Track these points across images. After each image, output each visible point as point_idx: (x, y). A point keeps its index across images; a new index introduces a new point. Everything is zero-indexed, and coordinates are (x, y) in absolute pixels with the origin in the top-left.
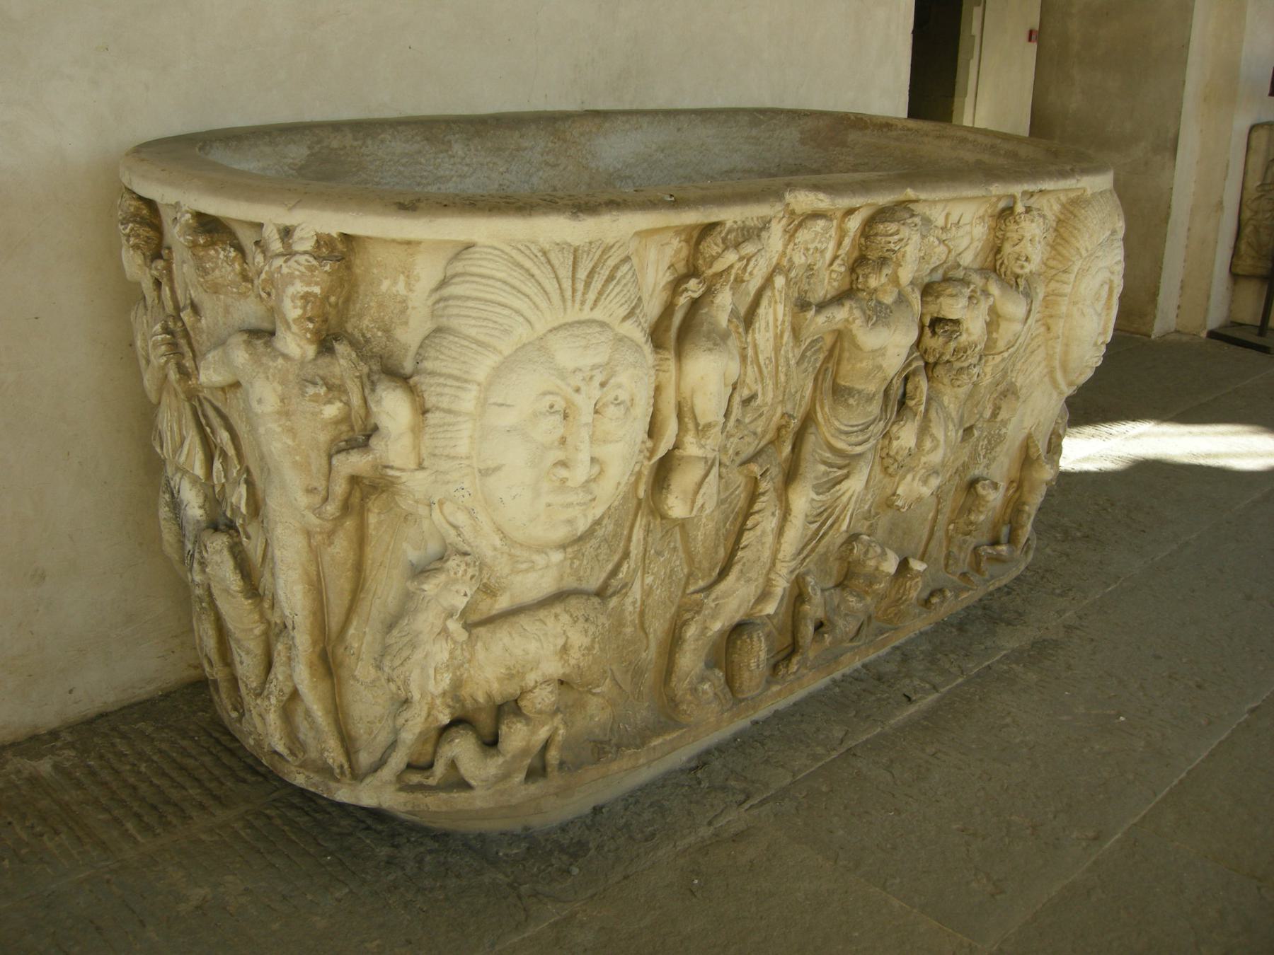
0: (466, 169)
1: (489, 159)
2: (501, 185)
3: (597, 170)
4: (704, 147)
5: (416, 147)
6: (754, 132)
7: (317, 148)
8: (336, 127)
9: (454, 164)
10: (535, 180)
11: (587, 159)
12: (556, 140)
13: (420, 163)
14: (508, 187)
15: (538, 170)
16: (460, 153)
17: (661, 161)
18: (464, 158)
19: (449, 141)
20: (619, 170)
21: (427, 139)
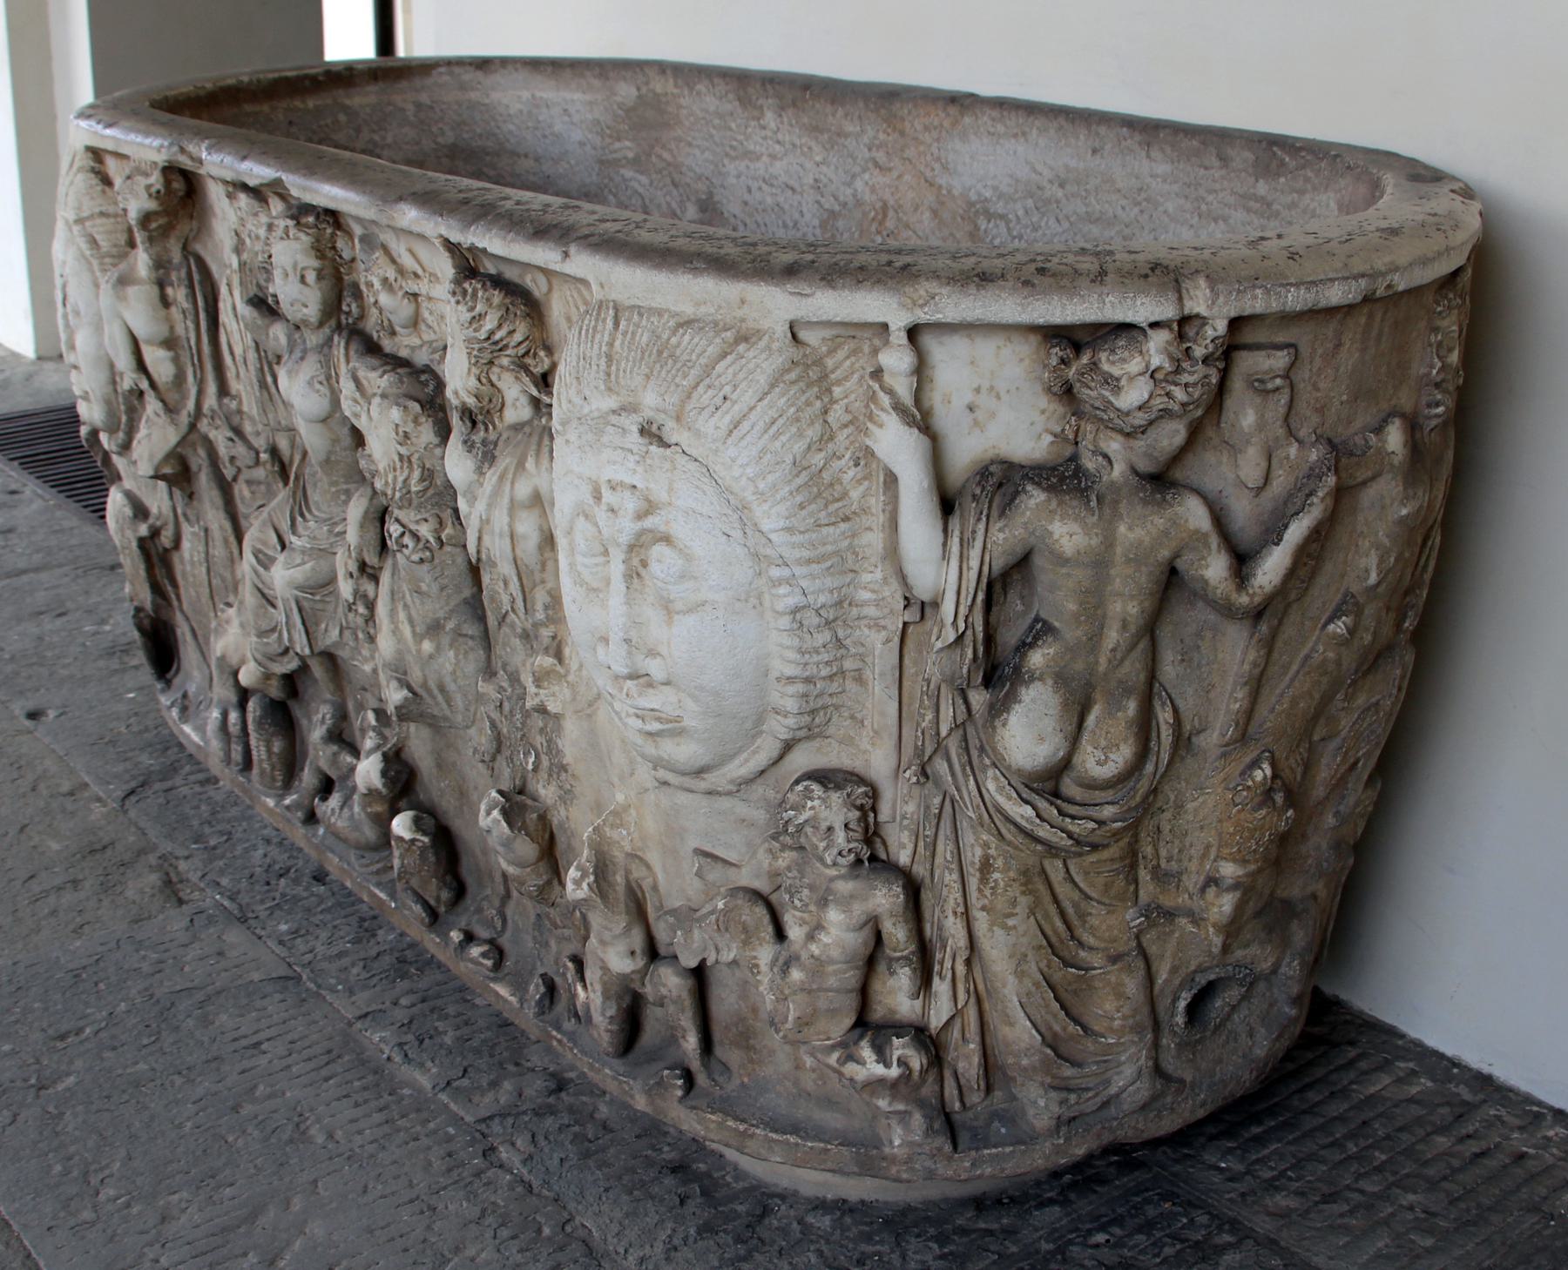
0: (777, 147)
1: (803, 141)
2: (816, 180)
3: (949, 192)
4: (1143, 195)
5: (729, 107)
6: (1262, 188)
7: (644, 90)
8: (662, 67)
9: (765, 138)
10: (859, 184)
11: (933, 170)
12: (889, 130)
13: (730, 129)
14: (825, 186)
15: (864, 171)
16: (773, 125)
17: (1058, 202)
18: (776, 133)
19: (761, 107)
20: (986, 200)
21: (739, 100)
